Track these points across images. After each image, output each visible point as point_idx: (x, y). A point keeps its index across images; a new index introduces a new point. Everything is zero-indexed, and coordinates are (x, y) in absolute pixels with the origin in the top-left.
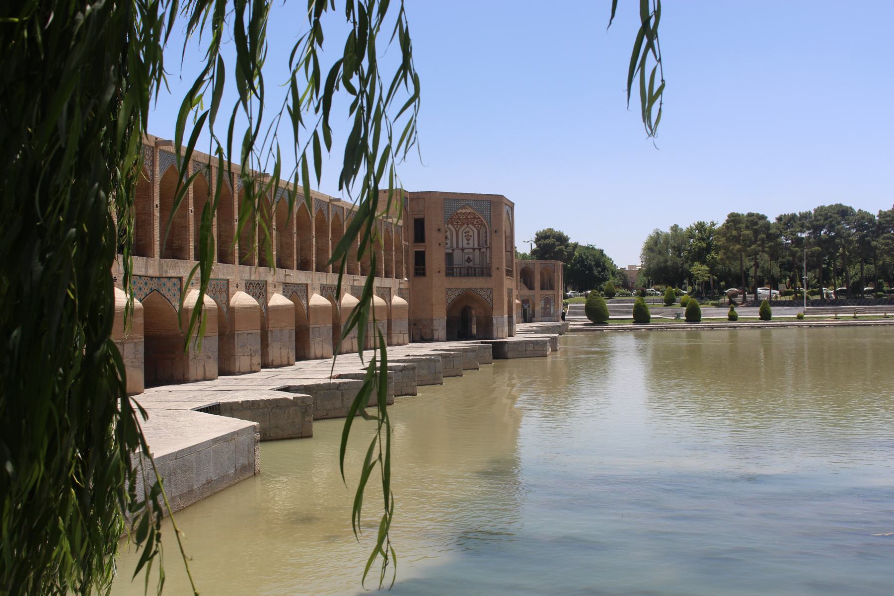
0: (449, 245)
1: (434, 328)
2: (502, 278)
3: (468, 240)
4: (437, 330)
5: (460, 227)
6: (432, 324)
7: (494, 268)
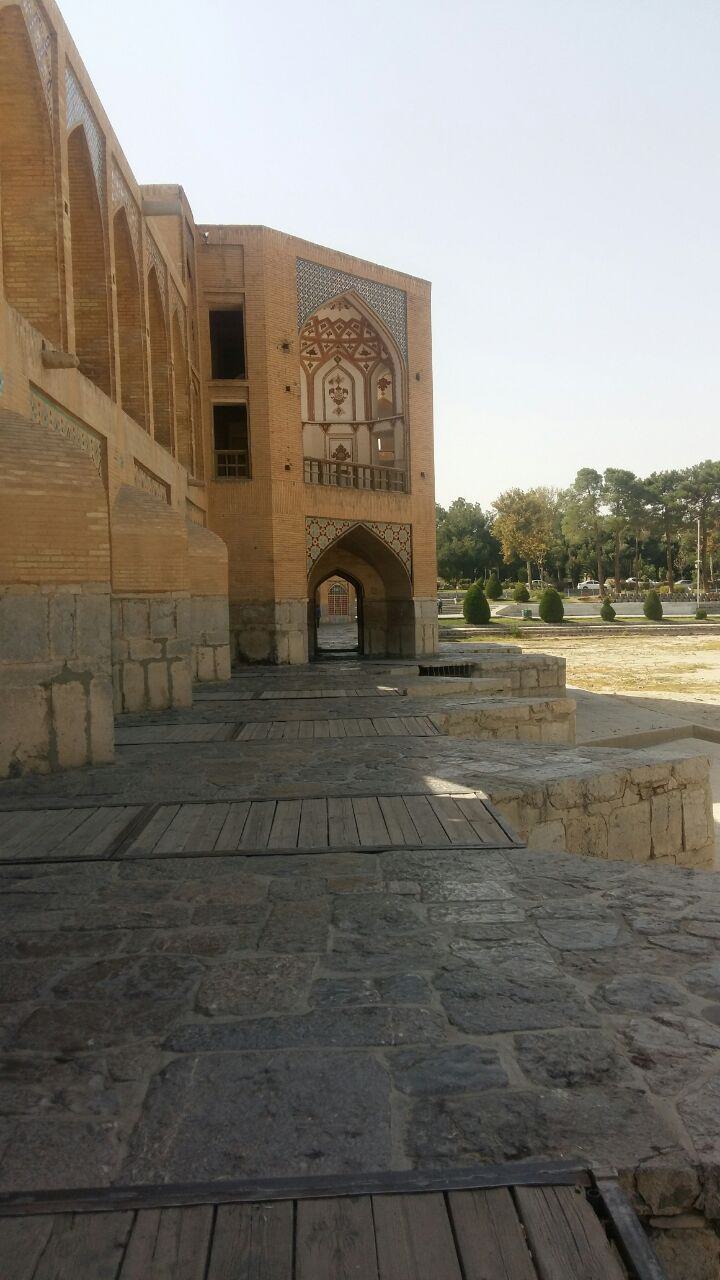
1: (278, 627)
3: (339, 402)
4: (285, 633)
5: (318, 368)
6: (271, 618)
7: (415, 475)
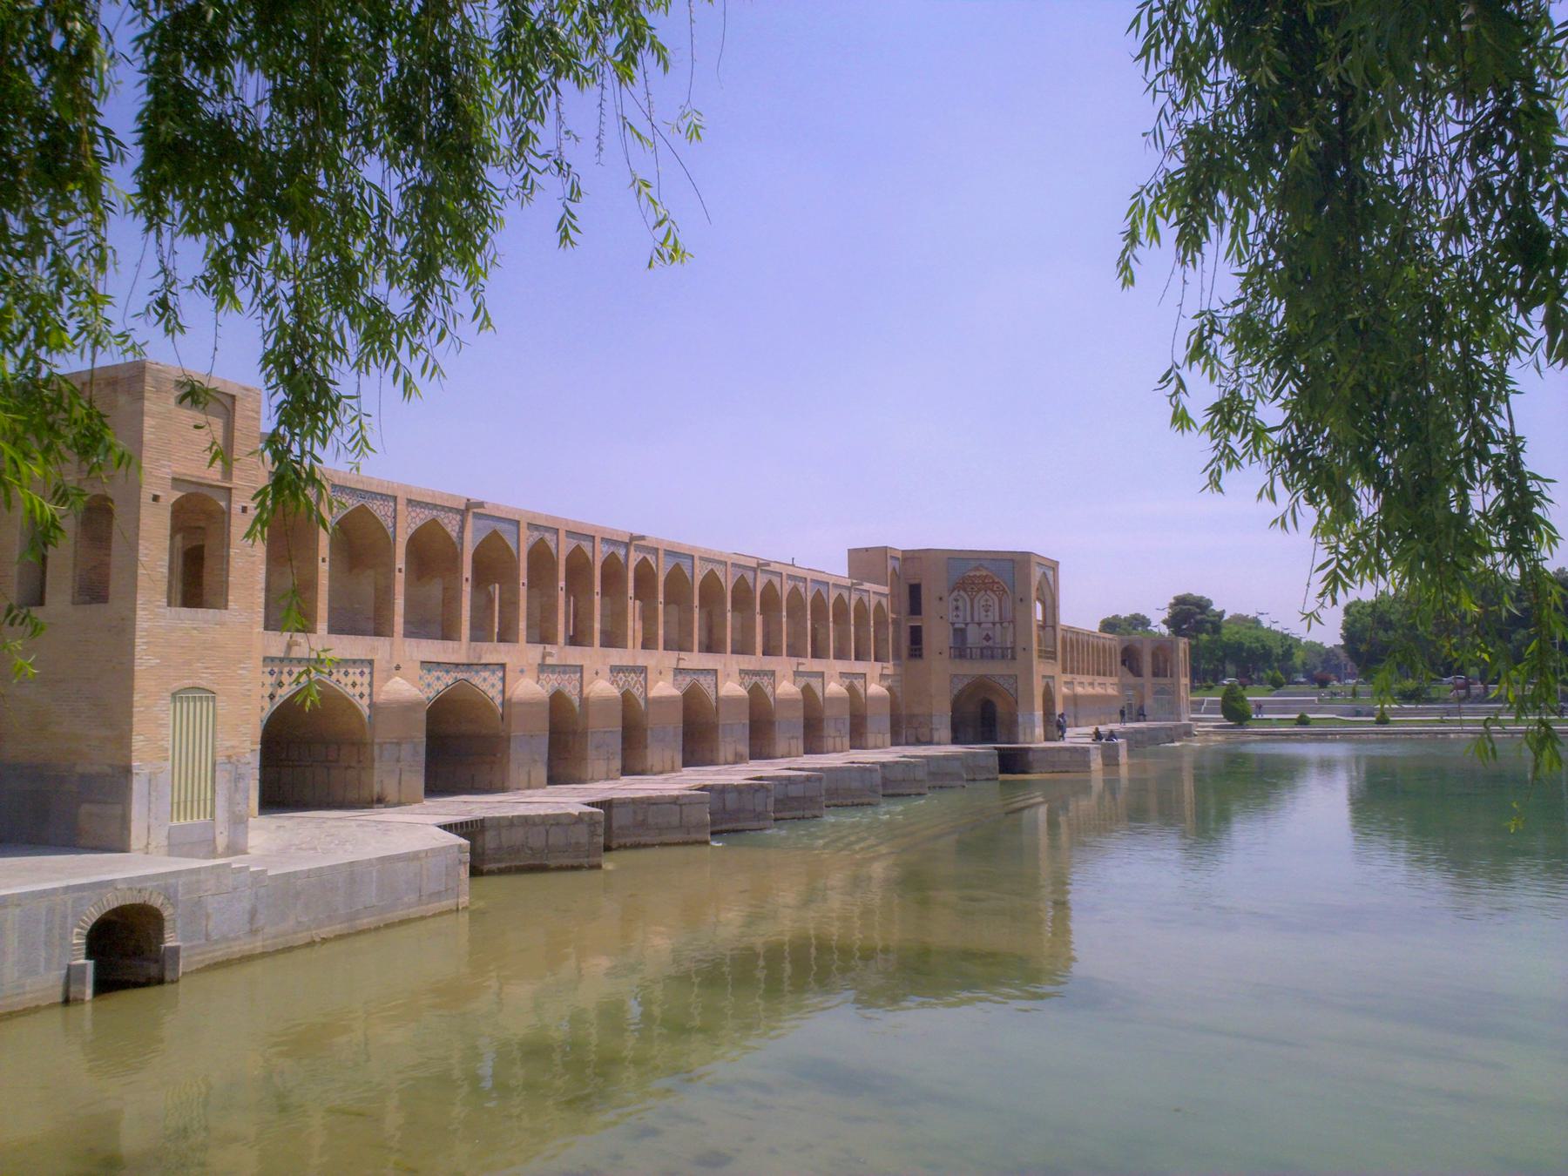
0: (961, 619)
2: (1031, 661)
3: (987, 611)
